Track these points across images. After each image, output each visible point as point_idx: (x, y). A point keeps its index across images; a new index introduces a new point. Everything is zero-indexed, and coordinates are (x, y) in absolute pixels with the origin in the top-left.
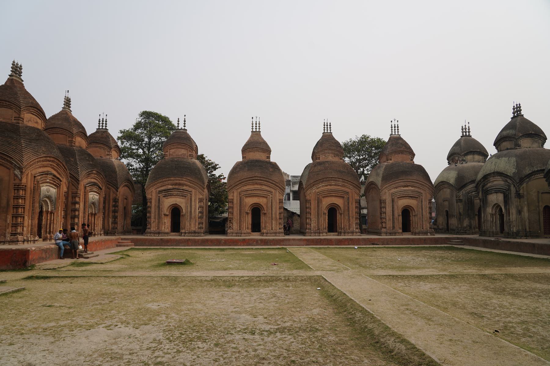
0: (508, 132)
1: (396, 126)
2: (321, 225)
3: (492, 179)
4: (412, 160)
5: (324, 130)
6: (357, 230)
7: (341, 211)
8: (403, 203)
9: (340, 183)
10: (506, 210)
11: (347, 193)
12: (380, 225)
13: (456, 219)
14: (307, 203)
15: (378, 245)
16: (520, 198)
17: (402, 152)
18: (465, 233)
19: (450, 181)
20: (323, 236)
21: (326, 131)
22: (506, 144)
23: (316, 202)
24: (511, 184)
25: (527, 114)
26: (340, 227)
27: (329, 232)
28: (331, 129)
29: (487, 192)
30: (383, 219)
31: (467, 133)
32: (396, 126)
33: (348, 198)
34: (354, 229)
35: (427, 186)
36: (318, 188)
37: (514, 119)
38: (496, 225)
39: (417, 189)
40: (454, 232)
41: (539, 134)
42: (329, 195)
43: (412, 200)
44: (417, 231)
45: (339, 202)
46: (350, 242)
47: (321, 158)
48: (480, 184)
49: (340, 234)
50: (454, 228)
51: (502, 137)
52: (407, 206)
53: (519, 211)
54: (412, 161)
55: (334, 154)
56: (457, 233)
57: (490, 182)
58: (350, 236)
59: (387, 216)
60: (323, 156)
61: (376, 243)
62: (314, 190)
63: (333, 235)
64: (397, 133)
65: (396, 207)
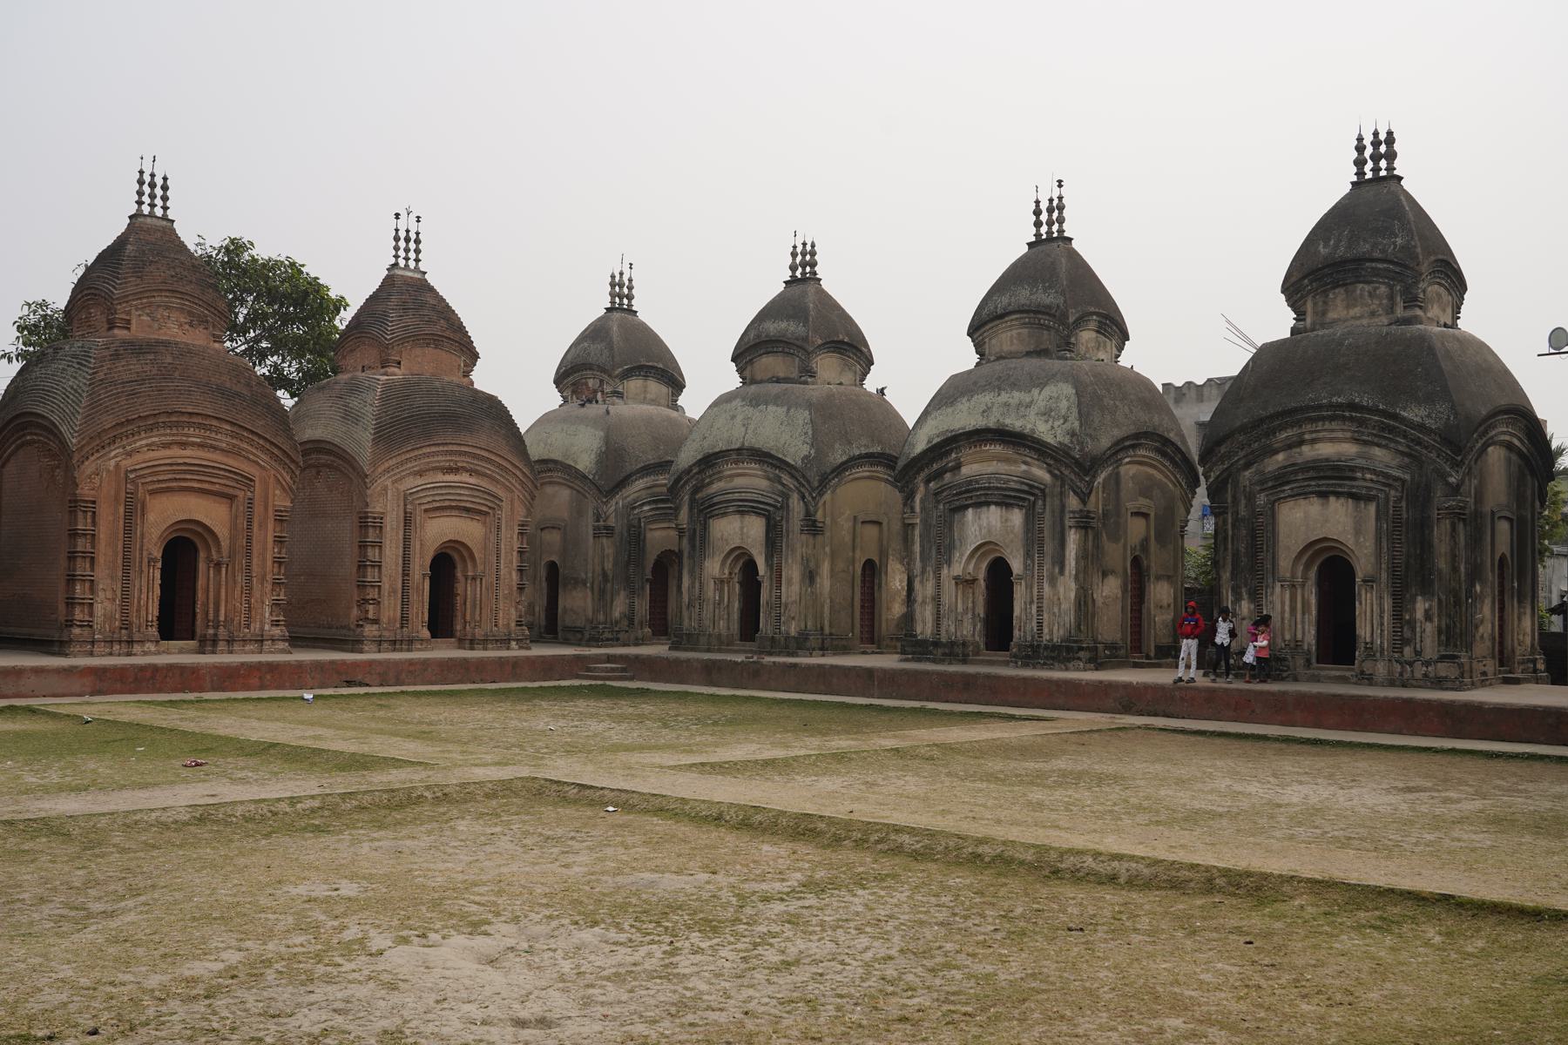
0: (783, 325)
1: (413, 236)
2: (138, 611)
3: (729, 469)
4: (467, 374)
5: (140, 203)
6: (277, 631)
7: (219, 551)
8: (438, 530)
9: (221, 441)
10: (771, 569)
11: (248, 481)
12: (355, 612)
13: (589, 593)
14: (80, 515)
15: (367, 685)
16: (815, 535)
17: (436, 341)
18: (615, 641)
19: (576, 462)
20: (145, 653)
21: (146, 209)
22: (770, 364)
23: (122, 510)
24: (790, 489)
25: (834, 280)
26: (211, 616)
27: (163, 639)
28: (168, 204)
29: (707, 510)
30: (369, 590)
31: (626, 301)
32: (413, 236)
33: (251, 501)
34: (267, 627)
35: (518, 473)
36: (129, 454)
37: (797, 289)
38: (728, 614)
39: (484, 483)
40: (579, 636)
41: (859, 346)
42: (174, 484)
43: (469, 522)
44: (479, 633)
45: (212, 514)
46: (268, 677)
47: (134, 321)
48: (686, 482)
49: (208, 644)
50: (580, 623)
51: (763, 338)
52: (450, 541)
53: (810, 572)
54: (466, 380)
55: (190, 313)
56: (589, 640)
57: (720, 479)
58: (253, 652)
59: (385, 579)
60: (145, 318)
61: (359, 678)
62: (114, 458)
63: (181, 651)
64: (412, 264)
65: (416, 546)
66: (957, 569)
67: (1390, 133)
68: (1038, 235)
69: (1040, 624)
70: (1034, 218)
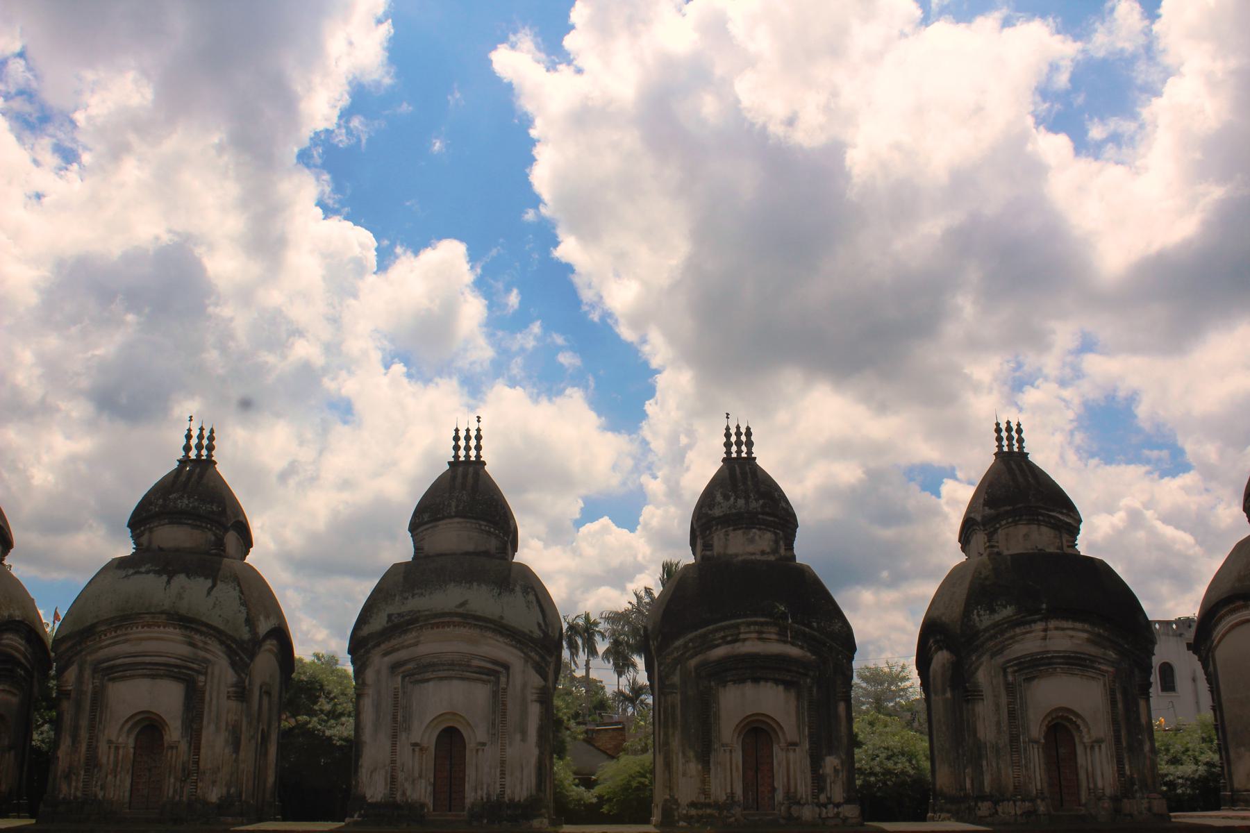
57: (126, 641)
66: (416, 736)
67: (748, 429)
68: (456, 456)
69: (503, 786)
70: (453, 443)
